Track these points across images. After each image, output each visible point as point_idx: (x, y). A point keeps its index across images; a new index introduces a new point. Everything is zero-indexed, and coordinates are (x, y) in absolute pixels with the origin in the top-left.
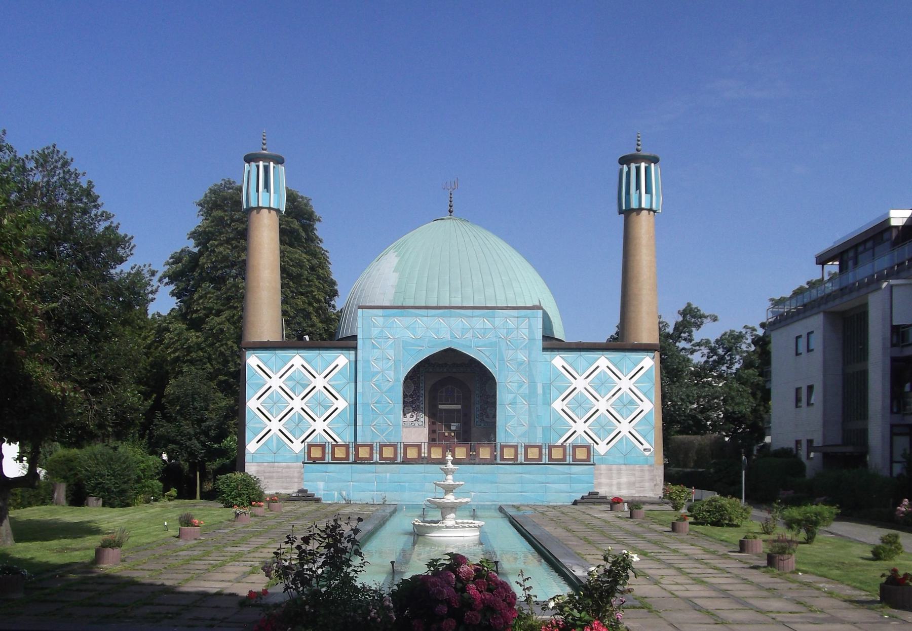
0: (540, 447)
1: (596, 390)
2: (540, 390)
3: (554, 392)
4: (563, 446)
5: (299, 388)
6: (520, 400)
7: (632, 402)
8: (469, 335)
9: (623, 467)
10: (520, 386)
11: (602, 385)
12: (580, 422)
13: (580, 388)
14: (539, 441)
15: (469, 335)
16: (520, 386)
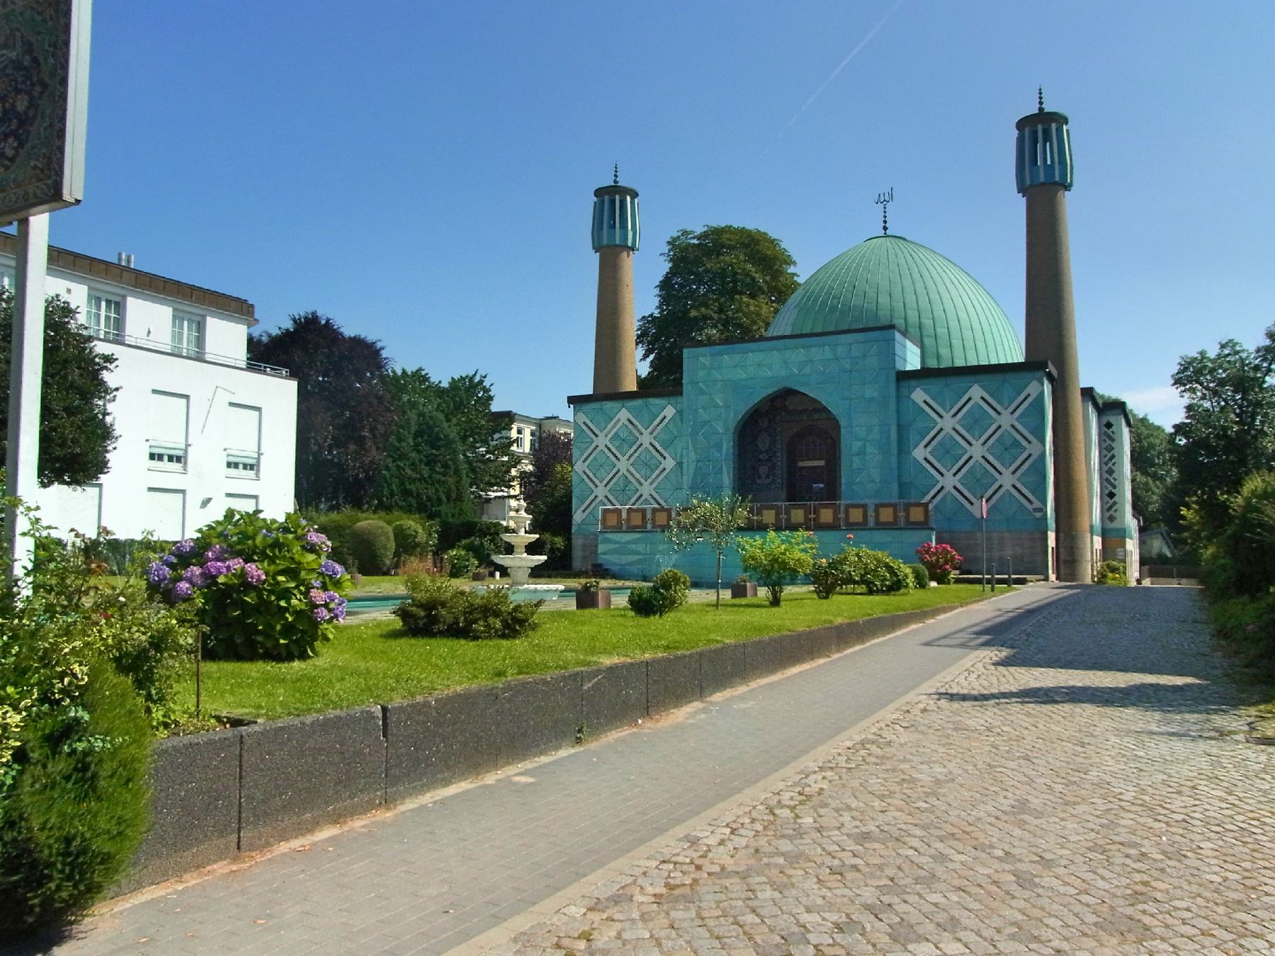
0: (894, 506)
1: (968, 431)
2: (894, 436)
3: (913, 436)
4: (926, 505)
5: (626, 447)
6: (870, 449)
7: (1016, 444)
8: (807, 370)
9: (1007, 535)
10: (869, 430)
11: (976, 422)
12: (949, 475)
13: (948, 429)
14: (895, 500)
15: (807, 370)
16: (869, 430)
